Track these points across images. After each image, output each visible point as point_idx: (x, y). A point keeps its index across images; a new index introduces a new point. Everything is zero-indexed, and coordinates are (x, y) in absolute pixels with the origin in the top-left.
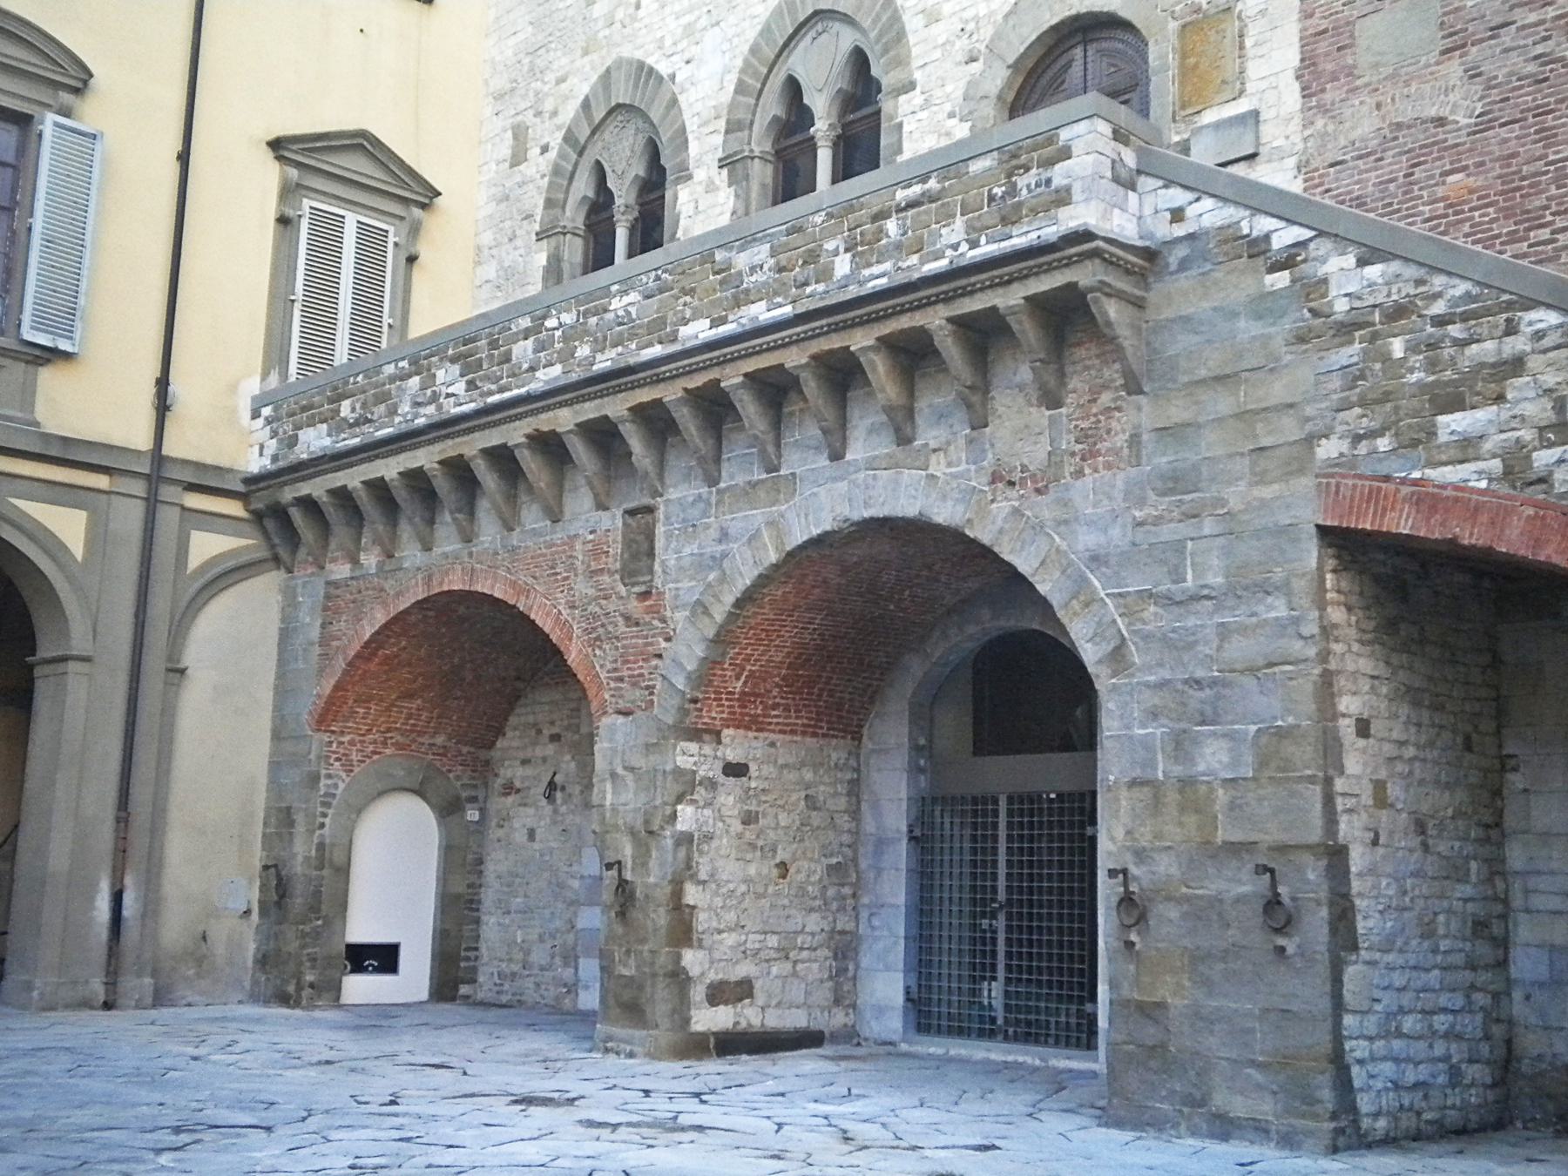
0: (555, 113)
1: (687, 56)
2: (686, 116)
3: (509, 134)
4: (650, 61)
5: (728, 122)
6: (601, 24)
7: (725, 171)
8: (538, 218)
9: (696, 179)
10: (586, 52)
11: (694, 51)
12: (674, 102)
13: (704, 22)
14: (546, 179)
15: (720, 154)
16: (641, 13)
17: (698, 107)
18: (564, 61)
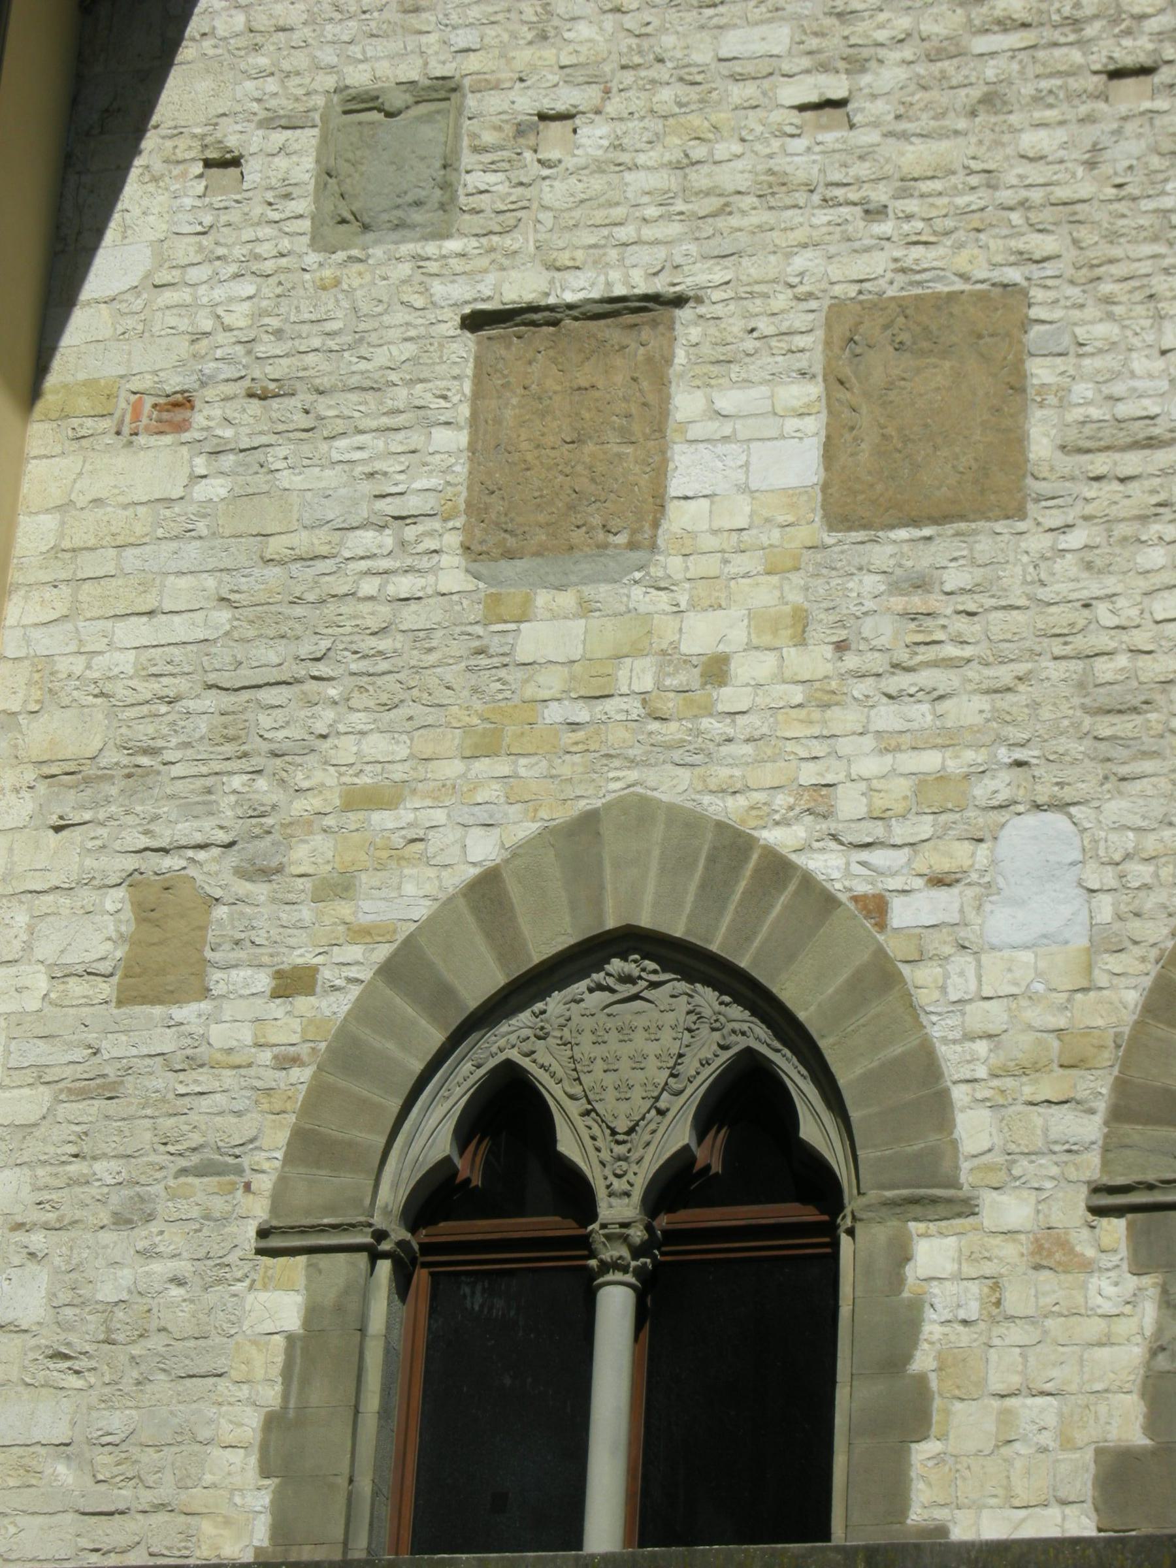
0: (338, 887)
1: (943, 865)
2: (939, 1029)
3: (116, 899)
4: (772, 836)
5: (1122, 1086)
6: (551, 682)
7: (1116, 1229)
8: (265, 1183)
9: (988, 1218)
10: (485, 746)
11: (959, 855)
12: (882, 977)
13: (1000, 785)
14: (302, 1075)
15: (1091, 1167)
16: (729, 697)
17: (995, 1015)
18: (377, 746)
